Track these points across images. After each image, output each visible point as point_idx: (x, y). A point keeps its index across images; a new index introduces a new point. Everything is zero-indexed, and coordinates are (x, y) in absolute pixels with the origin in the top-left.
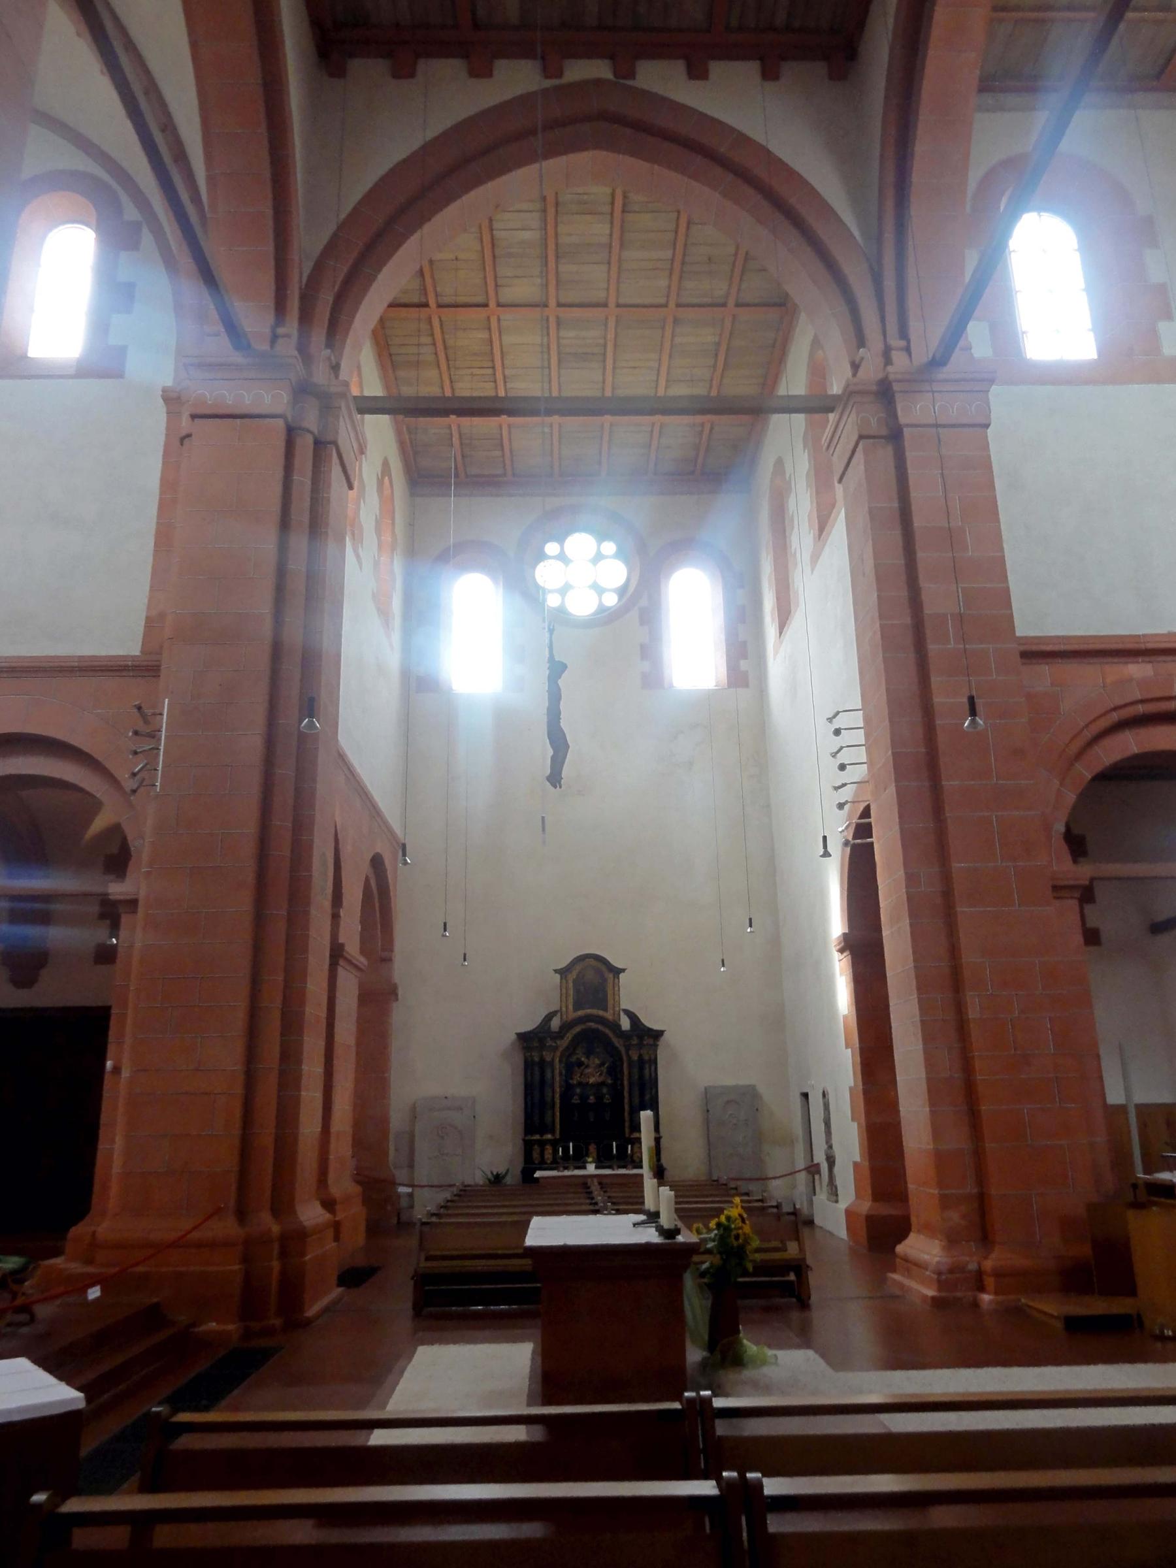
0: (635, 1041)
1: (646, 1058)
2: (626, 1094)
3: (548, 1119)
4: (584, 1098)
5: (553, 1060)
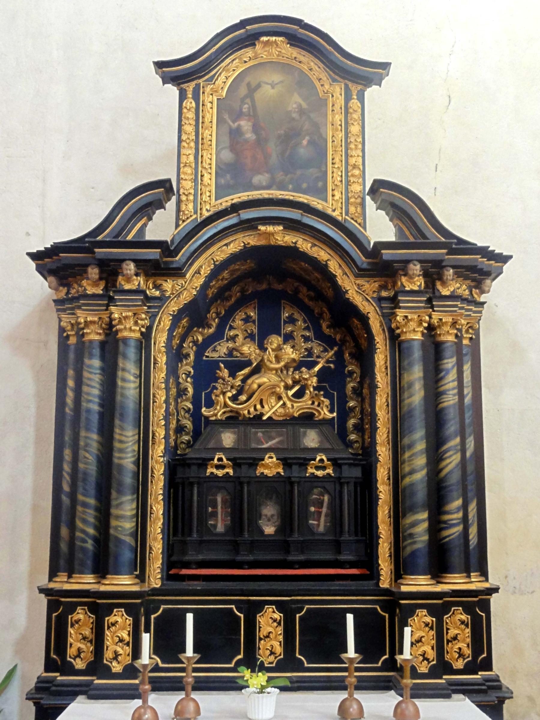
1: (448, 337)
3: (124, 523)
4: (246, 461)
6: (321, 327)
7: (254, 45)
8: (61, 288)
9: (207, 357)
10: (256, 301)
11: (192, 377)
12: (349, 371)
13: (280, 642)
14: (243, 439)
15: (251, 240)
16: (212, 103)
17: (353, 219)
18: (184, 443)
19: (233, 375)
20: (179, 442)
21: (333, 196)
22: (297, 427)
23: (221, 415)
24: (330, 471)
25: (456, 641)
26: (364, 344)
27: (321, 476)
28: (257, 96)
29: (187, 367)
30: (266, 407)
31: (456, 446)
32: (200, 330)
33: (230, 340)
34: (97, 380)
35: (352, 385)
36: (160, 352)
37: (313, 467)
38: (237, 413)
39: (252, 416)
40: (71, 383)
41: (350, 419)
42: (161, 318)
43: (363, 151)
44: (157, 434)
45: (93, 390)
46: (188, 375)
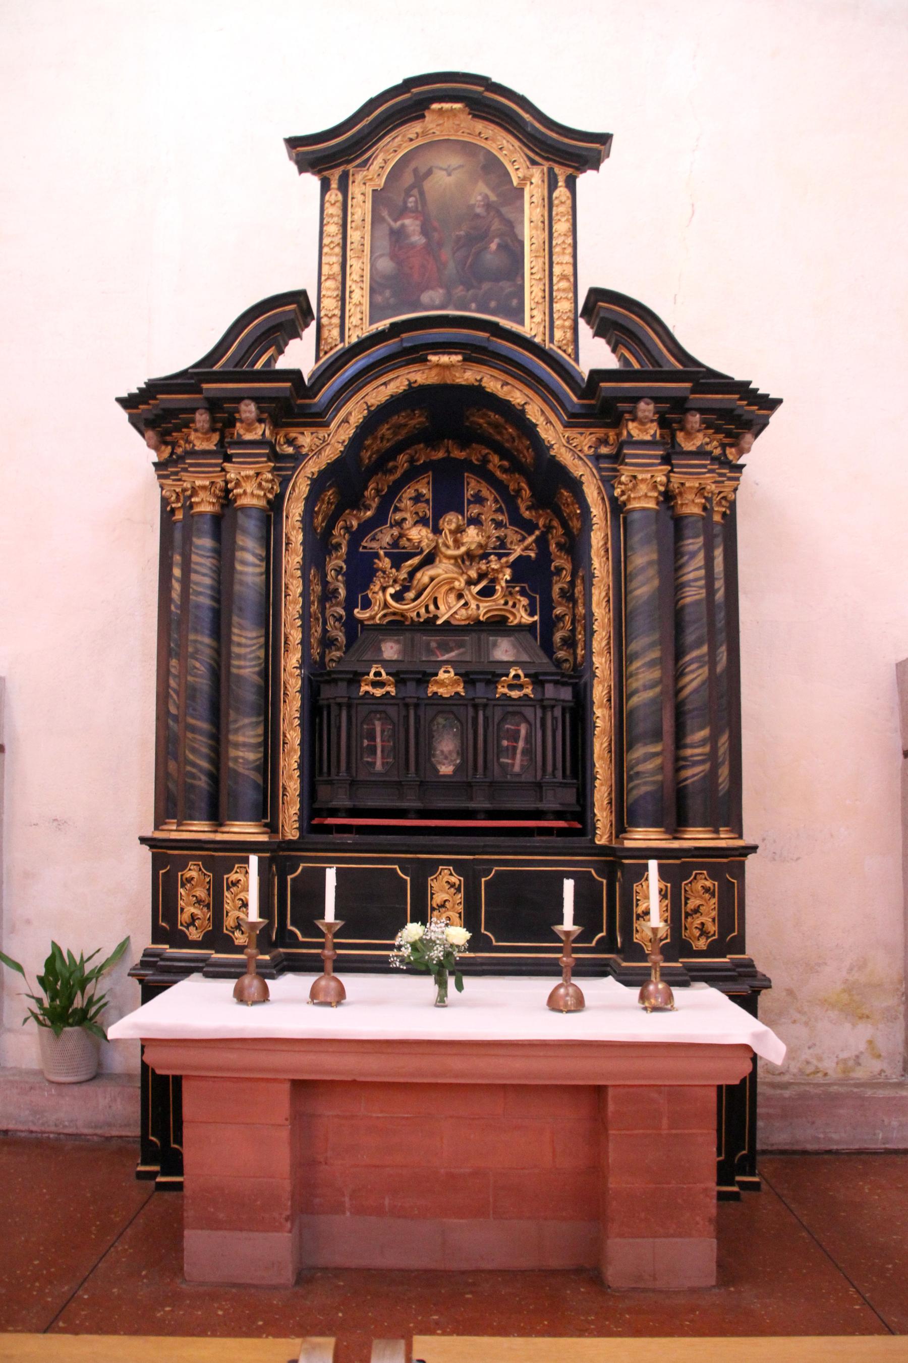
0: (642, 429)
2: (602, 664)
5: (274, 509)
6: (518, 508)
7: (423, 116)
8: (163, 447)
9: (365, 547)
10: (430, 473)
11: (343, 575)
12: (556, 567)
13: (460, 914)
14: (409, 649)
15: (420, 376)
16: (363, 194)
17: (560, 348)
18: (335, 661)
19: (397, 565)
20: (327, 659)
21: (532, 317)
22: (483, 636)
23: (380, 619)
24: (528, 691)
25: (698, 915)
26: (576, 524)
27: (516, 697)
28: (427, 185)
29: (336, 562)
30: (442, 607)
31: (703, 656)
32: (355, 512)
33: (395, 526)
34: (208, 564)
35: (560, 585)
36: (294, 528)
37: (505, 685)
38: (403, 615)
39: (422, 620)
40: (177, 572)
41: (558, 631)
42: (295, 483)
43: (575, 256)
44: (291, 638)
45: (203, 580)
46: (339, 571)
